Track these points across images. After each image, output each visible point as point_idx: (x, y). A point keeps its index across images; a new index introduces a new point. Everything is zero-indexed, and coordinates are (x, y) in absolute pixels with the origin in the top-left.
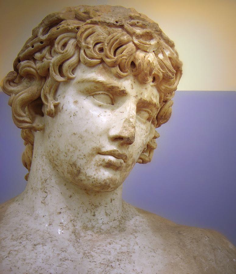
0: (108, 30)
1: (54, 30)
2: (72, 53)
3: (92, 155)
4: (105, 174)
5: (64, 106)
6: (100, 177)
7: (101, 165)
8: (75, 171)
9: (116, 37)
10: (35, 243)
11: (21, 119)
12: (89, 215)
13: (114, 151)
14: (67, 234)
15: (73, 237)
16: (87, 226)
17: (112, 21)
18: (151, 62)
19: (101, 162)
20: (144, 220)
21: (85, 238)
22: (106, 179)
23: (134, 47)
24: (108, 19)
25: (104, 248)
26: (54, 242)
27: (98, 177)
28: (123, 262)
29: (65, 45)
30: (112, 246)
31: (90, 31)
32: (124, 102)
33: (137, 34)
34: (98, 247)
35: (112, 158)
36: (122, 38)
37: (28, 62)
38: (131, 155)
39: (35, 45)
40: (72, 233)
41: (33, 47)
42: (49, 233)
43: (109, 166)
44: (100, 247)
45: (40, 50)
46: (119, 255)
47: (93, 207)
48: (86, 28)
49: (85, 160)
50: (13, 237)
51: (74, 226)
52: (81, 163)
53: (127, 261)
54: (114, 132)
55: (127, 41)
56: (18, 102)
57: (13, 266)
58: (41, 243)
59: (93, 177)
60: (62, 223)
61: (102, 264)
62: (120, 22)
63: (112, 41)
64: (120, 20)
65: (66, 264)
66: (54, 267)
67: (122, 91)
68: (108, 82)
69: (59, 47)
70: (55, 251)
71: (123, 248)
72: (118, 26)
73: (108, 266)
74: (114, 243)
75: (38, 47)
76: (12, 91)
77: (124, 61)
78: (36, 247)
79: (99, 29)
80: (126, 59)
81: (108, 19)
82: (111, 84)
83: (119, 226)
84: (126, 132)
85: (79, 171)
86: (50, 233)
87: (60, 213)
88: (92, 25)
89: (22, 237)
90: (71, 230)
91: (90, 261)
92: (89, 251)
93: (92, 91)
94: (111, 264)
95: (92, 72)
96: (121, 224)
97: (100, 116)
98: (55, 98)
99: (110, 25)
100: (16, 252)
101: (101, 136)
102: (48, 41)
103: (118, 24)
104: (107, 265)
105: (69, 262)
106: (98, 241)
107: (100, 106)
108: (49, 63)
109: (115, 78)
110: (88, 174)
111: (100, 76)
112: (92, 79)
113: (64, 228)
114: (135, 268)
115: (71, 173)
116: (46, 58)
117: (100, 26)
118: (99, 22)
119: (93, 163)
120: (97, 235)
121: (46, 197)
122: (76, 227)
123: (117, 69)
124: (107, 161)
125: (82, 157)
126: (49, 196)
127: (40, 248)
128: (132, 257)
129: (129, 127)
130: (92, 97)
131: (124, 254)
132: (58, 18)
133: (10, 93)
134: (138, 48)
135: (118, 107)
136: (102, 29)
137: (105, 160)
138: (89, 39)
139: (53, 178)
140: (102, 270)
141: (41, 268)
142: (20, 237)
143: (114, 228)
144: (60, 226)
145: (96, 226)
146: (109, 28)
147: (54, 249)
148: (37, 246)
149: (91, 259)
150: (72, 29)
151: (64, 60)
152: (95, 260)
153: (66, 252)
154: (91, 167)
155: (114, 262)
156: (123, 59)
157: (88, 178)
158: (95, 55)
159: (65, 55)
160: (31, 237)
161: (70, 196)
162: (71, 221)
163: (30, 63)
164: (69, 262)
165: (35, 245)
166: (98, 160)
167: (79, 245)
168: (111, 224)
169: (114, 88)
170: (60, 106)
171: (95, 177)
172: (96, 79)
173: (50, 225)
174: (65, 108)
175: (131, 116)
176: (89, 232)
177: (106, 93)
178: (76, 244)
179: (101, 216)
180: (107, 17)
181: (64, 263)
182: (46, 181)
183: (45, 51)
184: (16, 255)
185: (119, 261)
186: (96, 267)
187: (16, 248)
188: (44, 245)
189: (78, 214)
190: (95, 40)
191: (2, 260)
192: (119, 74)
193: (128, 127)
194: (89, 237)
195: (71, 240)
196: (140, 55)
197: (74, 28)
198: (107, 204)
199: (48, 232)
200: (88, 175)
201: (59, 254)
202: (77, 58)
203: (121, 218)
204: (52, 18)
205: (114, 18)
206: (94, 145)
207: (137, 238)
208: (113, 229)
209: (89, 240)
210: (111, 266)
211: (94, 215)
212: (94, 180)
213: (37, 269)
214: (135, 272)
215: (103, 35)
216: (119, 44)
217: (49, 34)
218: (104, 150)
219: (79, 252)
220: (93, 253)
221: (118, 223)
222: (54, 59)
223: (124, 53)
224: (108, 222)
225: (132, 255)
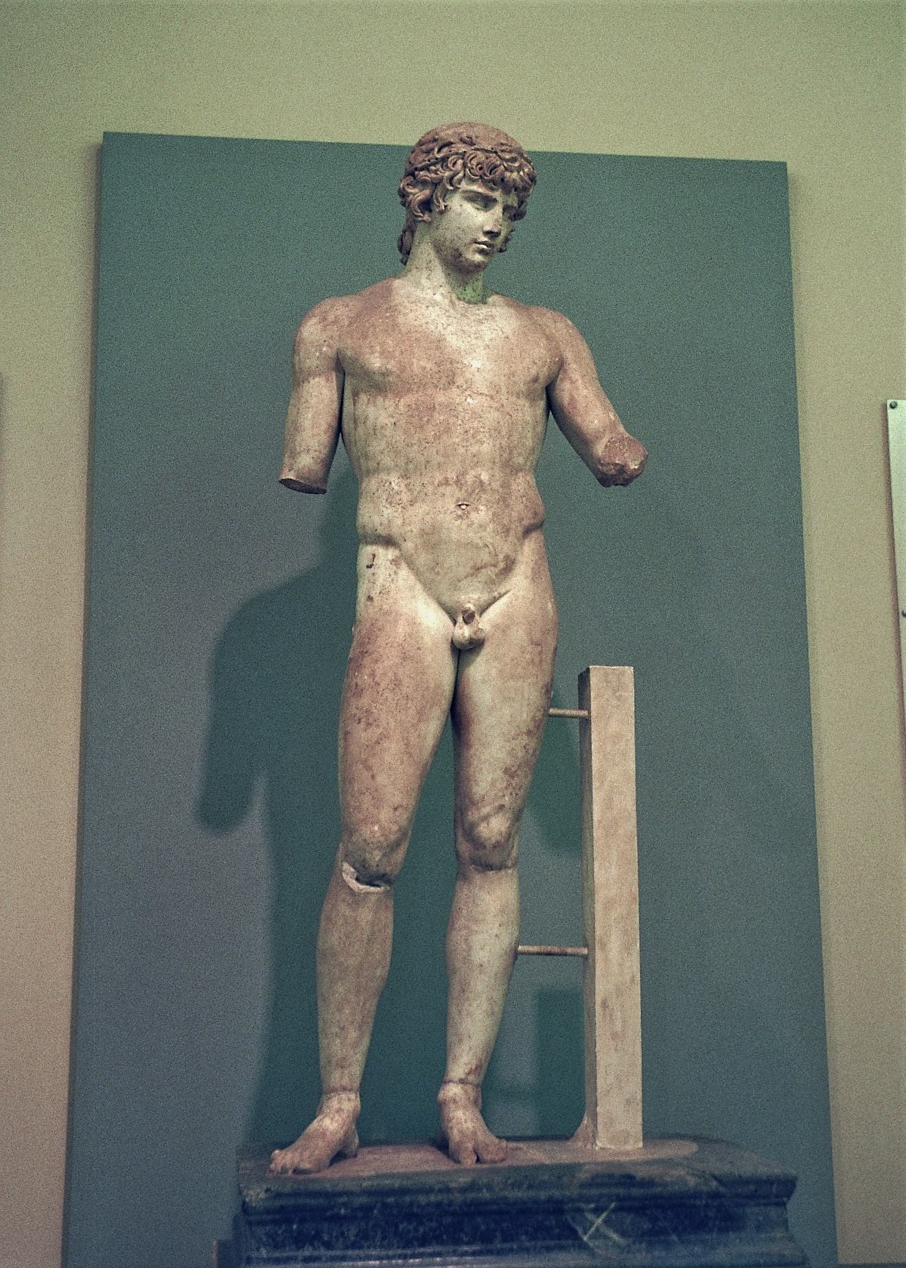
1: (445, 149)
3: (470, 244)
4: (478, 258)
12: (461, 289)
14: (447, 301)
17: (489, 148)
29: (455, 164)
43: (481, 252)
45: (434, 164)
52: (462, 249)
54: (487, 228)
93: (473, 198)
123: (491, 184)
134: (506, 169)
179: (469, 290)
183: (439, 166)
196: (508, 174)
222: (447, 174)
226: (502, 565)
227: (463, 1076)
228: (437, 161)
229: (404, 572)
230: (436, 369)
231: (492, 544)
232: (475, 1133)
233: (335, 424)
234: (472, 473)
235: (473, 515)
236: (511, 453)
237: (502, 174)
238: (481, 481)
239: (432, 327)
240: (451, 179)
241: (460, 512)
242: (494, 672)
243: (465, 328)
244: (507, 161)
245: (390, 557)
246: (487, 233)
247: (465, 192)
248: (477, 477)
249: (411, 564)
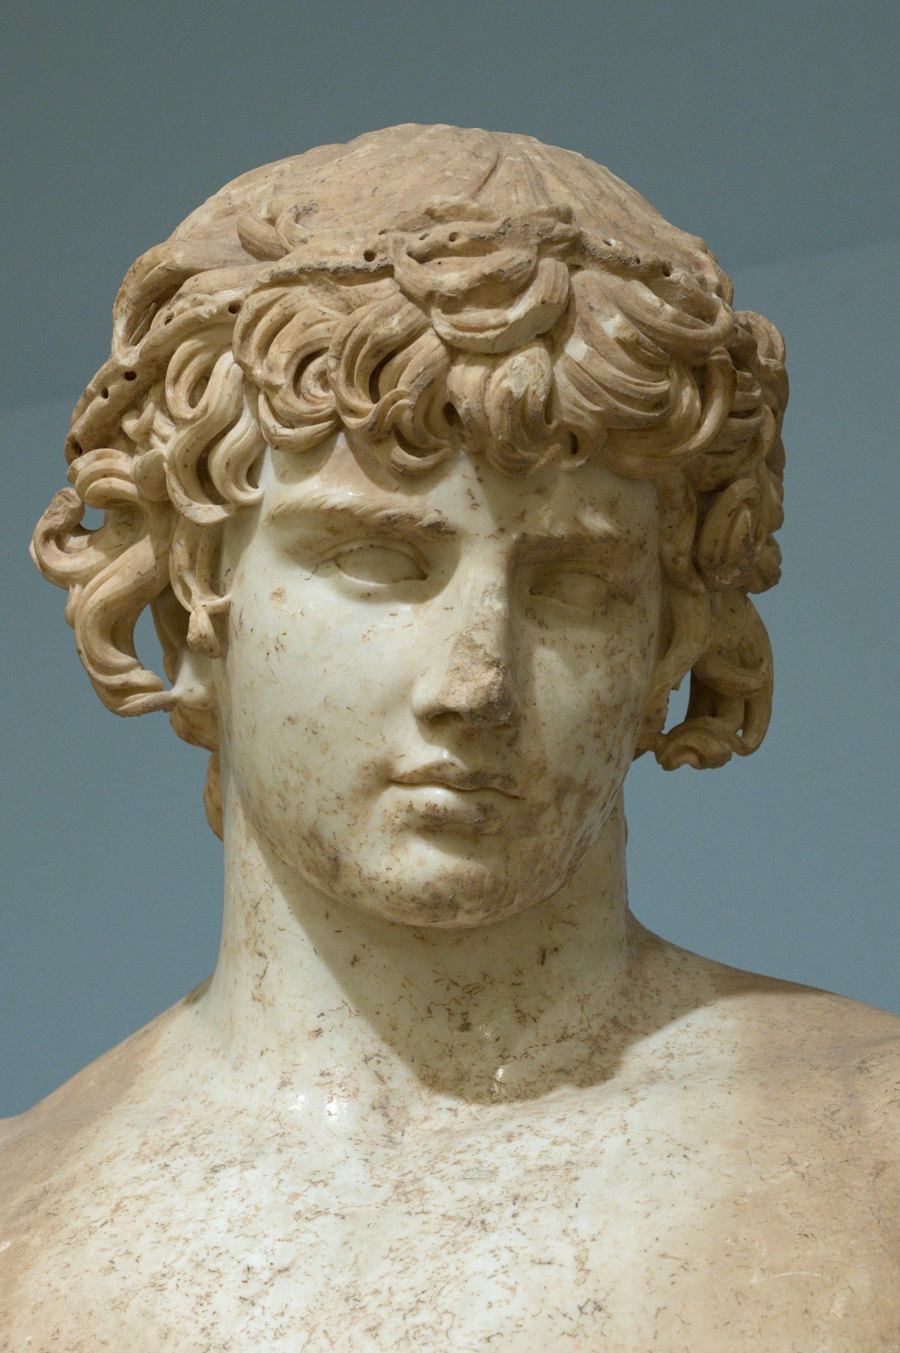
0: (343, 295)
2: (232, 410)
4: (424, 863)
5: (244, 612)
6: (407, 877)
7: (406, 827)
8: (323, 859)
9: (357, 332)
10: (218, 1162)
11: (116, 680)
13: (440, 766)
15: (376, 1123)
16: (435, 1075)
17: (350, 256)
18: (518, 391)
19: (403, 817)
20: (729, 1023)
21: (426, 1125)
22: (431, 879)
23: (442, 349)
24: (335, 253)
25: (480, 1156)
26: (291, 1150)
27: (400, 877)
28: (535, 1205)
30: (512, 1146)
31: (274, 313)
32: (454, 563)
33: (442, 296)
34: (459, 1157)
35: (438, 796)
36: (381, 331)
37: (99, 458)
38: (537, 763)
39: (111, 389)
40: (374, 1108)
41: (105, 394)
42: (277, 1120)
43: (433, 826)
44: (467, 1156)
46: (529, 1178)
47: (456, 992)
48: (258, 306)
49: (344, 818)
50: (145, 1148)
51: (381, 1079)
52: (333, 827)
53: (552, 1200)
54: (426, 694)
55: (405, 333)
56: (90, 618)
57: (122, 1252)
58: (239, 1158)
59: (382, 879)
60: (328, 1074)
61: (450, 1218)
62: (382, 251)
63: (349, 344)
64: (380, 247)
65: (314, 1229)
66: (268, 1242)
67: (429, 526)
68: (369, 505)
69: (181, 394)
70: (282, 1187)
71: (556, 1149)
72: (375, 271)
73: (470, 1223)
74: (528, 1135)
75: (120, 396)
76: (69, 573)
77: (407, 415)
78: (217, 1175)
79: (306, 300)
80: (411, 408)
81: (335, 253)
82: (381, 509)
83: (587, 1062)
84: (464, 689)
85: (336, 859)
86: (282, 1116)
87: (319, 1032)
88: (277, 291)
89: (177, 1144)
90: (365, 1100)
91: (409, 1213)
92: (419, 1175)
94: (482, 1217)
95: (309, 472)
96: (601, 1051)
97: (370, 635)
98: (215, 586)
99: (345, 276)
100: (141, 1203)
101: (384, 713)
102: (151, 366)
103: (373, 265)
104: (466, 1222)
105: (331, 1219)
106: (468, 1132)
107: (367, 597)
108: (160, 459)
109: (395, 483)
110: (364, 868)
111: (338, 486)
112: (307, 503)
113: (337, 1090)
114: (572, 1226)
115: (313, 867)
116: (157, 434)
117: (310, 286)
118: (302, 271)
119: (376, 820)
120: (474, 1108)
121: (265, 972)
122: (392, 1085)
124: (420, 808)
125: (333, 804)
126: (273, 968)
127: (229, 1179)
128: (578, 1183)
129: (474, 667)
130: (333, 567)
131: (547, 1175)
132: (168, 270)
133: (65, 581)
134: (455, 351)
135: (440, 587)
136: (319, 294)
137: (415, 806)
138: (274, 349)
139: (277, 893)
140: (442, 1241)
141: (216, 1252)
142: (167, 1146)
143: (560, 1070)
144: (318, 1084)
145: (475, 1070)
146: (343, 287)
147: (281, 1177)
148: (223, 1173)
149: (416, 1202)
150: (210, 312)
151: (204, 443)
152: (426, 1208)
153: (326, 1185)
154: (370, 840)
155: (496, 1209)
156: (402, 408)
157: (370, 884)
158: (301, 406)
159: (203, 425)
160: (210, 1138)
161: (351, 958)
162: (367, 1060)
163: (109, 460)
164: (331, 1219)
165: (214, 1170)
166: (391, 809)
167: (392, 1153)
168: (543, 1056)
169: (396, 522)
170: (234, 613)
171: (391, 876)
172: (323, 499)
173: (284, 1084)
175: (476, 619)
176: (445, 1102)
177: (376, 543)
178: (380, 1152)
180: (328, 246)
181: (308, 1225)
182: (256, 907)
184: (140, 1212)
185: (519, 1203)
186: (423, 1232)
187: (141, 1191)
188: (246, 1164)
189: (394, 1029)
190: (298, 350)
191: (87, 1236)
192: (401, 466)
193: (470, 668)
194: (442, 1120)
195: (362, 1136)
196: (466, 379)
197: (221, 312)
198: (520, 972)
199: (274, 1115)
200: (365, 872)
201: (295, 1196)
202: (254, 422)
203: (604, 1027)
204: (147, 273)
205: (357, 239)
206: (368, 754)
207: (640, 1105)
208: (552, 1076)
209: (441, 1131)
210: (483, 1222)
211: (466, 1027)
212: (388, 888)
213: (203, 1255)
214: (569, 1239)
215: (328, 320)
216: (375, 355)
217: (144, 341)
218: (404, 767)
219: (379, 1183)
220: (430, 1182)
221: (582, 1051)
222: (169, 442)
223: (401, 387)
224: (530, 1051)
225: (580, 1173)
237: (433, 385)
239: (176, 1303)
244: (452, 303)
246: (437, 719)
247: (285, 517)
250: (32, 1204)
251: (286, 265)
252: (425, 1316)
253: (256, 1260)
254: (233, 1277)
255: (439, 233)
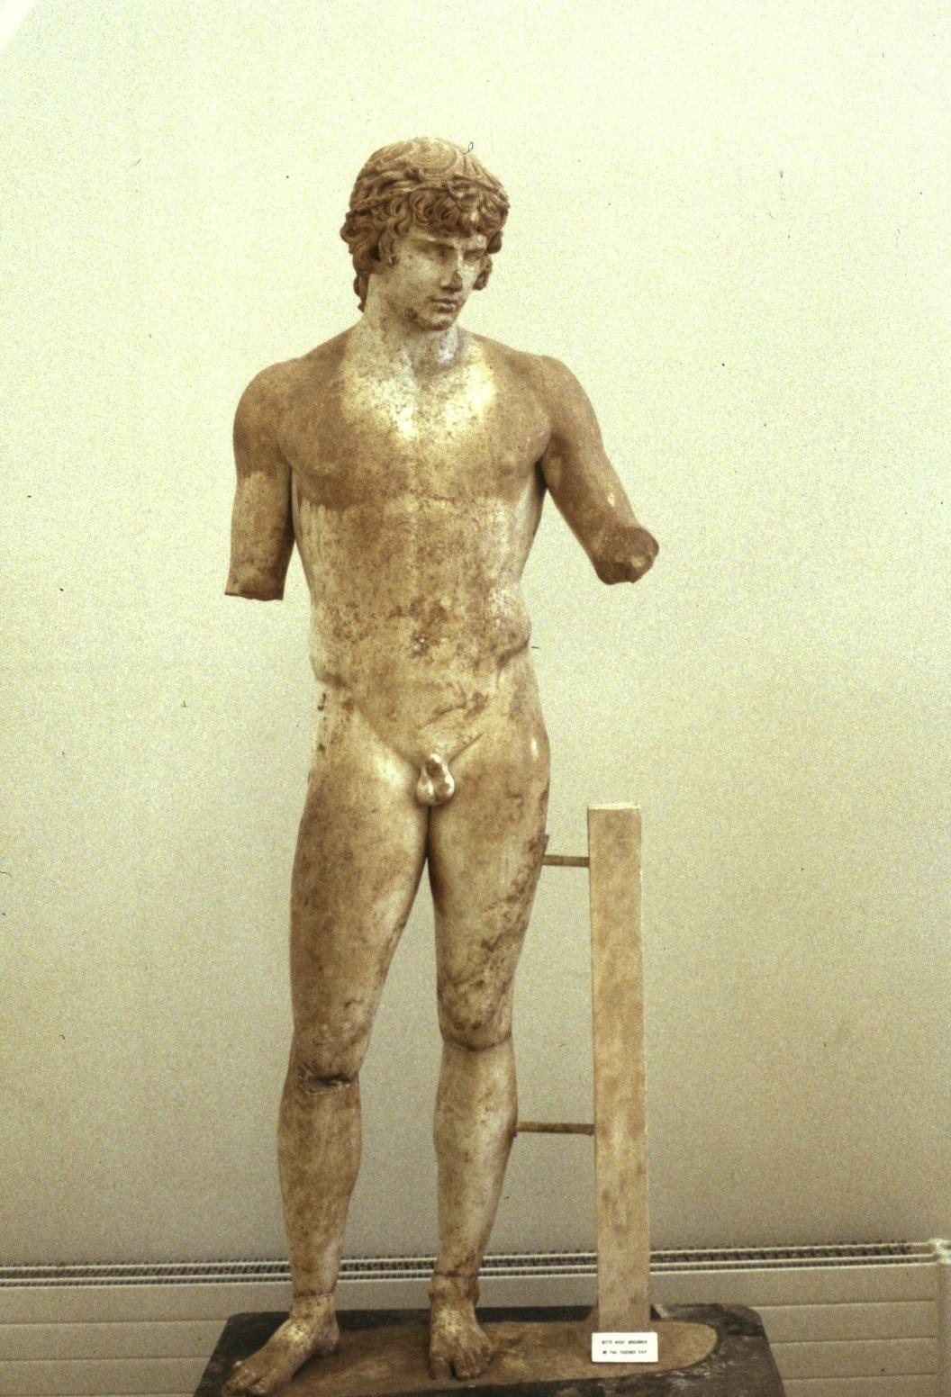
45: (376, 207)
54: (445, 283)
99: (438, 190)
123: (443, 231)
124: (439, 307)
127: (384, 383)
174: (401, 262)
187: (365, 384)
206: (428, 294)
220: (431, 387)
222: (391, 221)
226: (471, 705)
227: (453, 1269)
228: (378, 204)
229: (356, 718)
230: (383, 472)
231: (458, 682)
232: (456, 1339)
233: (283, 525)
234: (430, 599)
235: (434, 650)
236: (479, 567)
238: (441, 610)
239: (383, 413)
240: (396, 228)
241: (416, 647)
242: (464, 830)
243: (425, 408)
245: (341, 699)
248: (437, 603)
249: (363, 709)
250: (336, 385)
251: (423, 185)
252: (439, 418)
253: (398, 404)
254: (393, 408)
255: (458, 182)
